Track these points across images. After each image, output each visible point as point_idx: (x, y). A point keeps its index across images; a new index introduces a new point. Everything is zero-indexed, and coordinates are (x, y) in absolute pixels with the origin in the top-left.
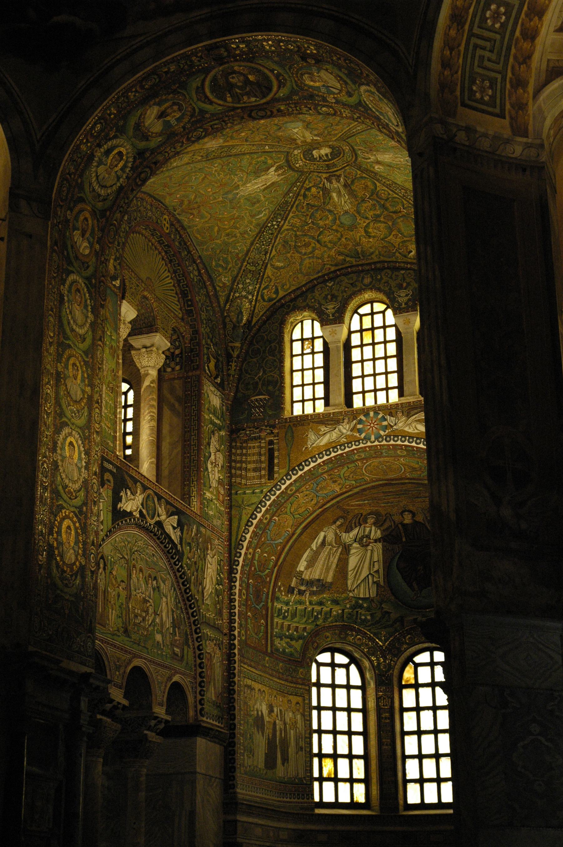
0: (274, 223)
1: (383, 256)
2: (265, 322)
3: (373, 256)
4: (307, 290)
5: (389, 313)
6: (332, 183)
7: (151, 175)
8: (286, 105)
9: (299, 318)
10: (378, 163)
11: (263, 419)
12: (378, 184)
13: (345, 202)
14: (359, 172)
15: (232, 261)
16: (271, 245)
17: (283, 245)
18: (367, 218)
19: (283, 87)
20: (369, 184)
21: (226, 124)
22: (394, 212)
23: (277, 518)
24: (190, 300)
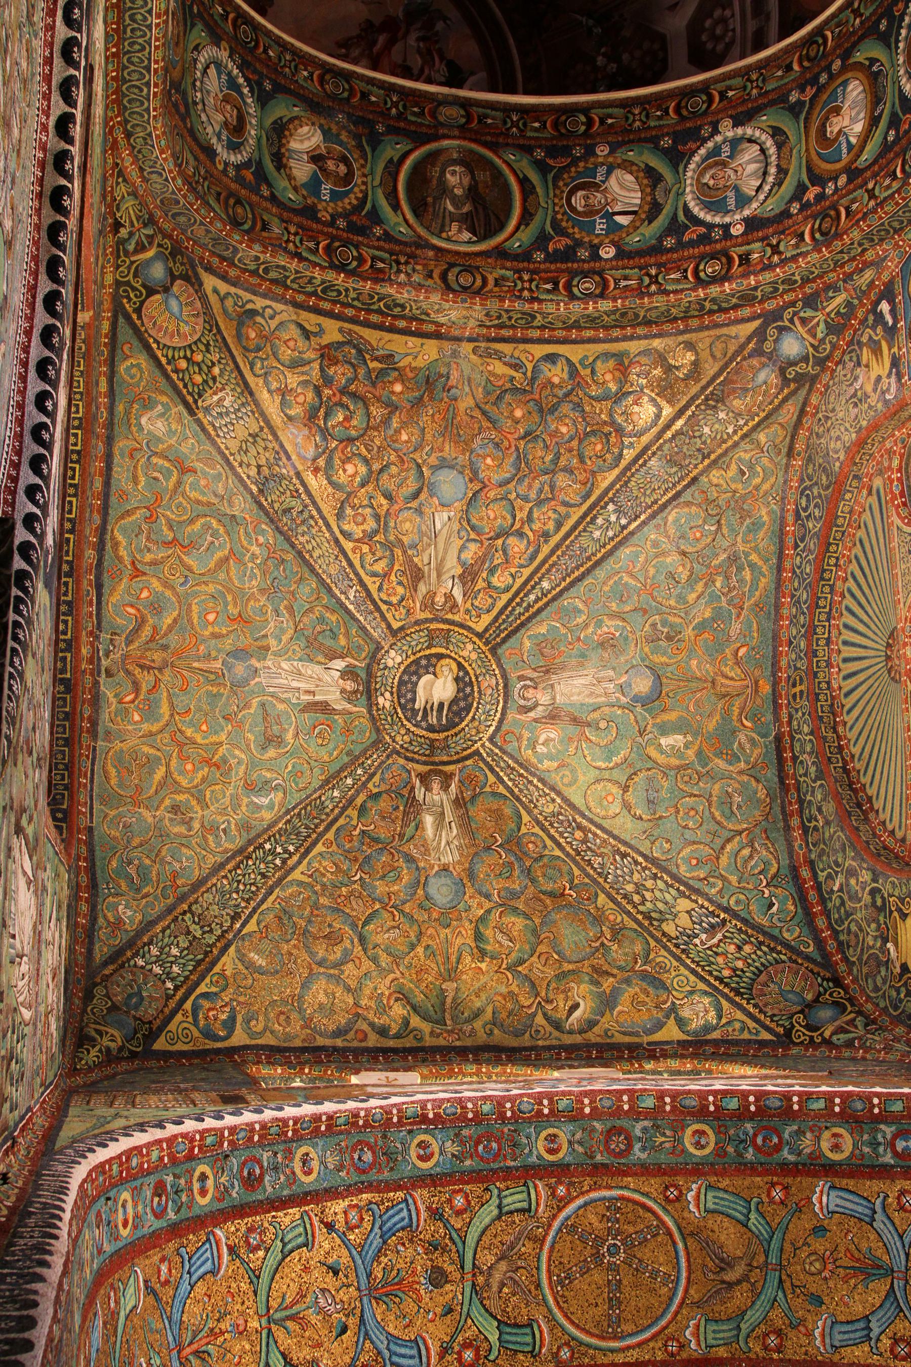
0: (279, 850)
3: (478, 1024)
6: (428, 789)
7: (247, 232)
8: (518, 271)
10: (553, 716)
13: (448, 843)
14: (492, 778)
16: (253, 904)
17: (280, 918)
18: (488, 896)
19: (527, 225)
20: (508, 811)
21: (399, 271)
22: (551, 894)
23: (226, 1257)
24: (64, 812)
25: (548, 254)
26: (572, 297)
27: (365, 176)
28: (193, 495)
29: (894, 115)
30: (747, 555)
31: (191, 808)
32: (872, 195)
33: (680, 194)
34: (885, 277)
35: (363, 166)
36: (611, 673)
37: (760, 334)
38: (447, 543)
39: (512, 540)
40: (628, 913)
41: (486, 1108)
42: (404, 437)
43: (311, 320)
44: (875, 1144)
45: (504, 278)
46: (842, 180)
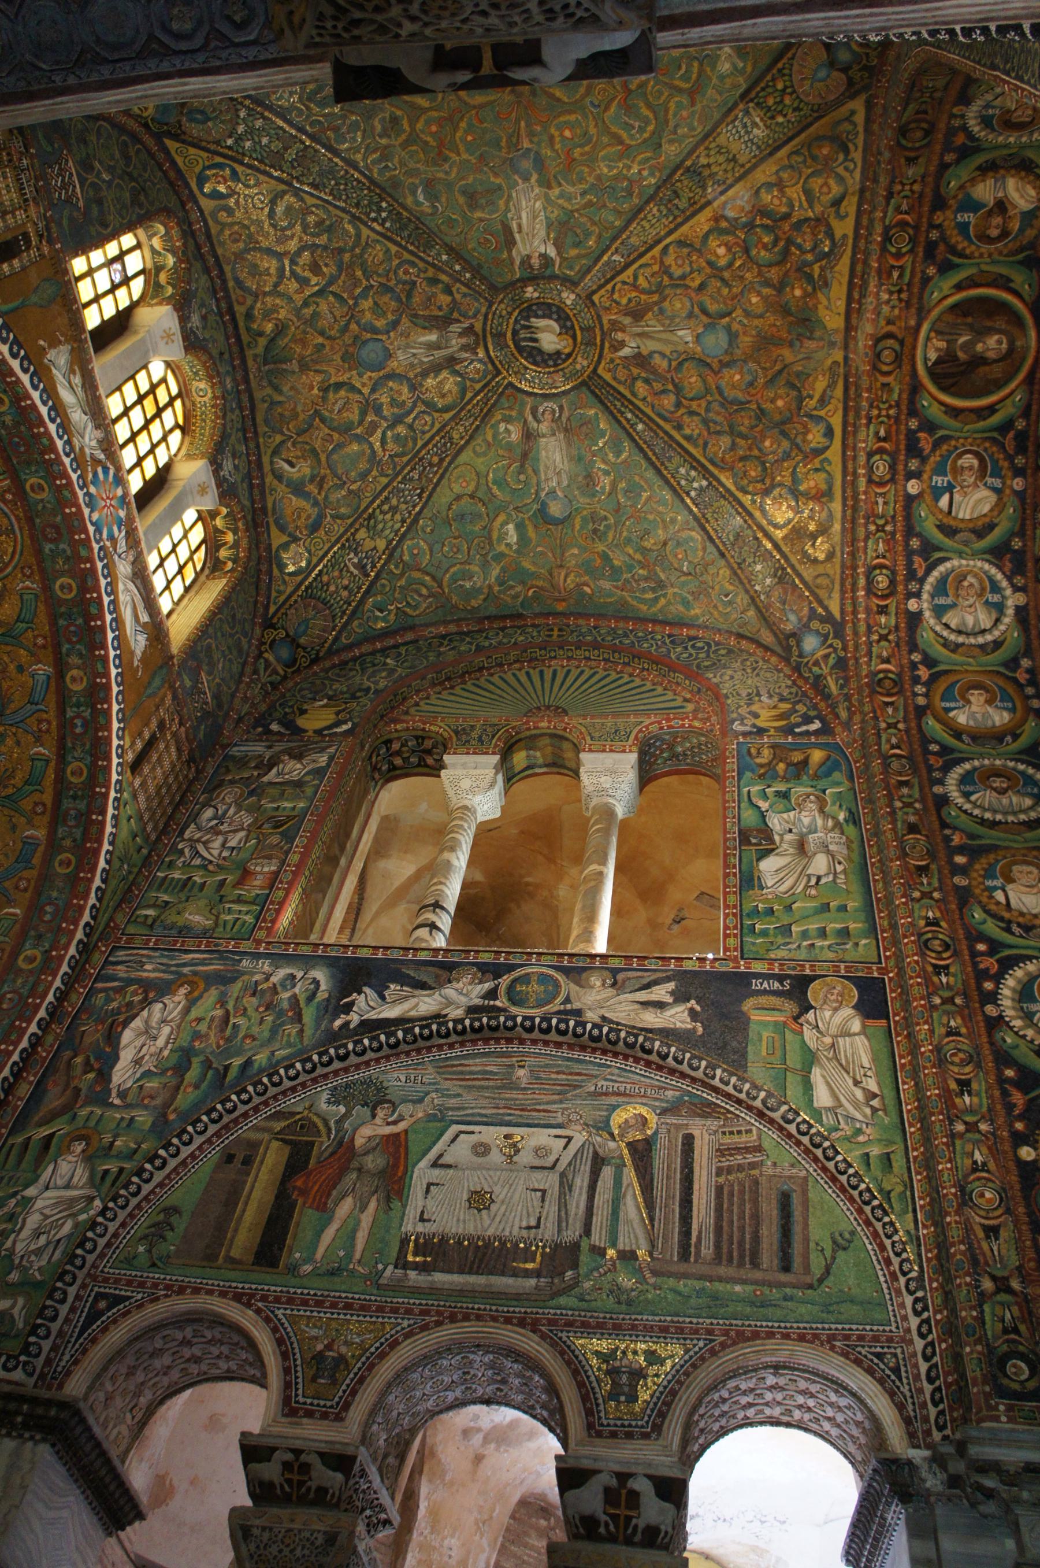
1: (270, 409)
2: (160, 166)
3: (269, 391)
4: (202, 257)
5: (177, 434)
6: (461, 335)
7: (898, 143)
8: (898, 405)
9: (156, 243)
10: (529, 436)
11: (51, 206)
12: (447, 416)
14: (478, 386)
15: (325, 116)
18: (373, 390)
21: (891, 293)
25: (915, 432)
26: (870, 455)
27: (990, 255)
28: (672, 105)
29: (952, 750)
30: (665, 596)
31: (398, 135)
32: (890, 726)
33: (961, 555)
34: (838, 729)
35: (1000, 253)
36: (565, 483)
37: (828, 618)
38: (666, 342)
39: (672, 398)
40: (372, 502)
41: (45, 441)
42: (754, 300)
43: (850, 206)
44: (78, 705)
45: (891, 391)
46: (921, 701)
